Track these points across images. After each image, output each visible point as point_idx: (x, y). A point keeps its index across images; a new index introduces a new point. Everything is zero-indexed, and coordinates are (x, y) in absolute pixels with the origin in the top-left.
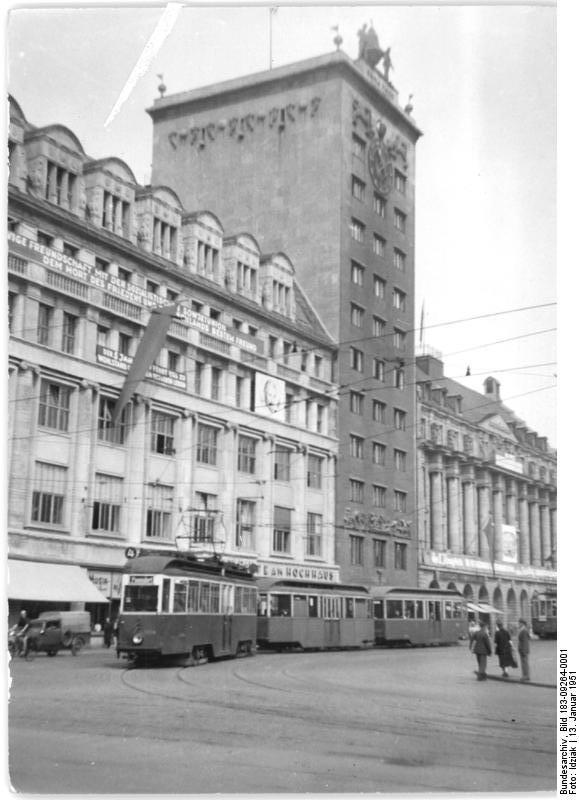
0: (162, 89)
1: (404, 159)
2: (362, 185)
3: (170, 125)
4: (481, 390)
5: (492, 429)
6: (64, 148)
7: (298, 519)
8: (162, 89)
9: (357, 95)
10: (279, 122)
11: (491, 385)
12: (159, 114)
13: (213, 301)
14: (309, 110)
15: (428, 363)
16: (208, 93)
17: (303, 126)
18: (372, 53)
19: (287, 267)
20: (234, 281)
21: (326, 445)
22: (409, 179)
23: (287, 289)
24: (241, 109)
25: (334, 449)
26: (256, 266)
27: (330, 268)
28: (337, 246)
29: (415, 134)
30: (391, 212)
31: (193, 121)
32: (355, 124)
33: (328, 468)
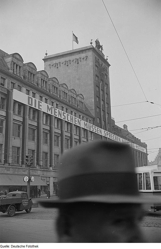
0: (46, 54)
1: (107, 71)
2: (98, 77)
3: (48, 63)
5: (128, 137)
6: (32, 68)
8: (46, 54)
10: (77, 62)
11: (125, 126)
12: (45, 60)
13: (66, 106)
14: (85, 58)
17: (84, 62)
18: (99, 46)
22: (108, 76)
24: (67, 59)
26: (76, 97)
27: (92, 98)
30: (105, 84)
31: (54, 61)
32: (96, 62)
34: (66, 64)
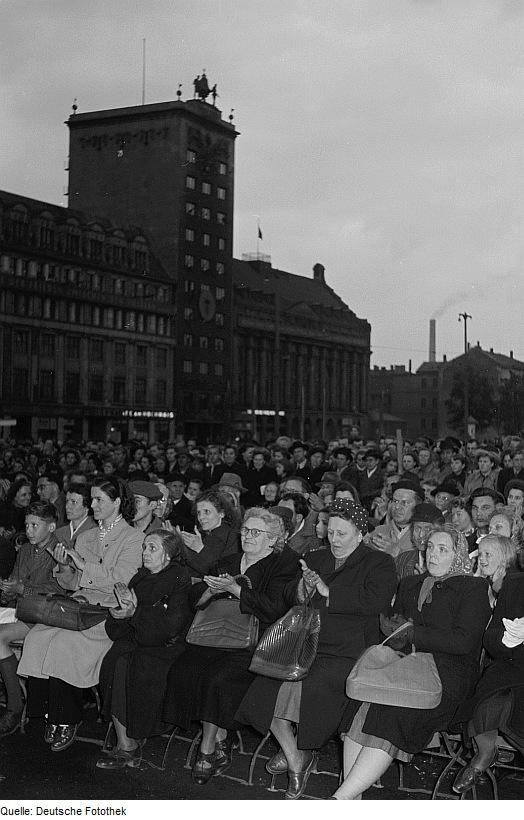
0: (75, 107)
4: (311, 275)
7: (151, 382)
8: (75, 107)
9: (191, 124)
11: (319, 269)
14: (163, 133)
21: (168, 341)
23: (145, 254)
33: (170, 356)
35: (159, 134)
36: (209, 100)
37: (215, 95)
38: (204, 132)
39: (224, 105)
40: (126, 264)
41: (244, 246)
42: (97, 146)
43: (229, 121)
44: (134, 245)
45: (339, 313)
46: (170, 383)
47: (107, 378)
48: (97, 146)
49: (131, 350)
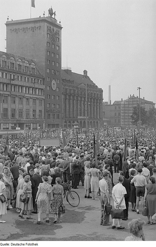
7: (37, 111)
10: (32, 30)
11: (85, 72)
15: (68, 72)
16: (17, 22)
19: (34, 64)
20: (24, 70)
21: (42, 97)
23: (34, 68)
24: (25, 26)
25: (44, 98)
28: (44, 57)
29: (61, 28)
31: (15, 27)
32: (47, 31)
33: (43, 102)
34: (24, 30)
35: (37, 28)
36: (53, 16)
37: (55, 15)
38: (52, 27)
39: (59, 18)
40: (29, 72)
41: (64, 65)
42: (16, 32)
43: (59, 23)
44: (31, 66)
45: (93, 86)
46: (43, 111)
47: (24, 110)
48: (16, 32)
49: (31, 100)
